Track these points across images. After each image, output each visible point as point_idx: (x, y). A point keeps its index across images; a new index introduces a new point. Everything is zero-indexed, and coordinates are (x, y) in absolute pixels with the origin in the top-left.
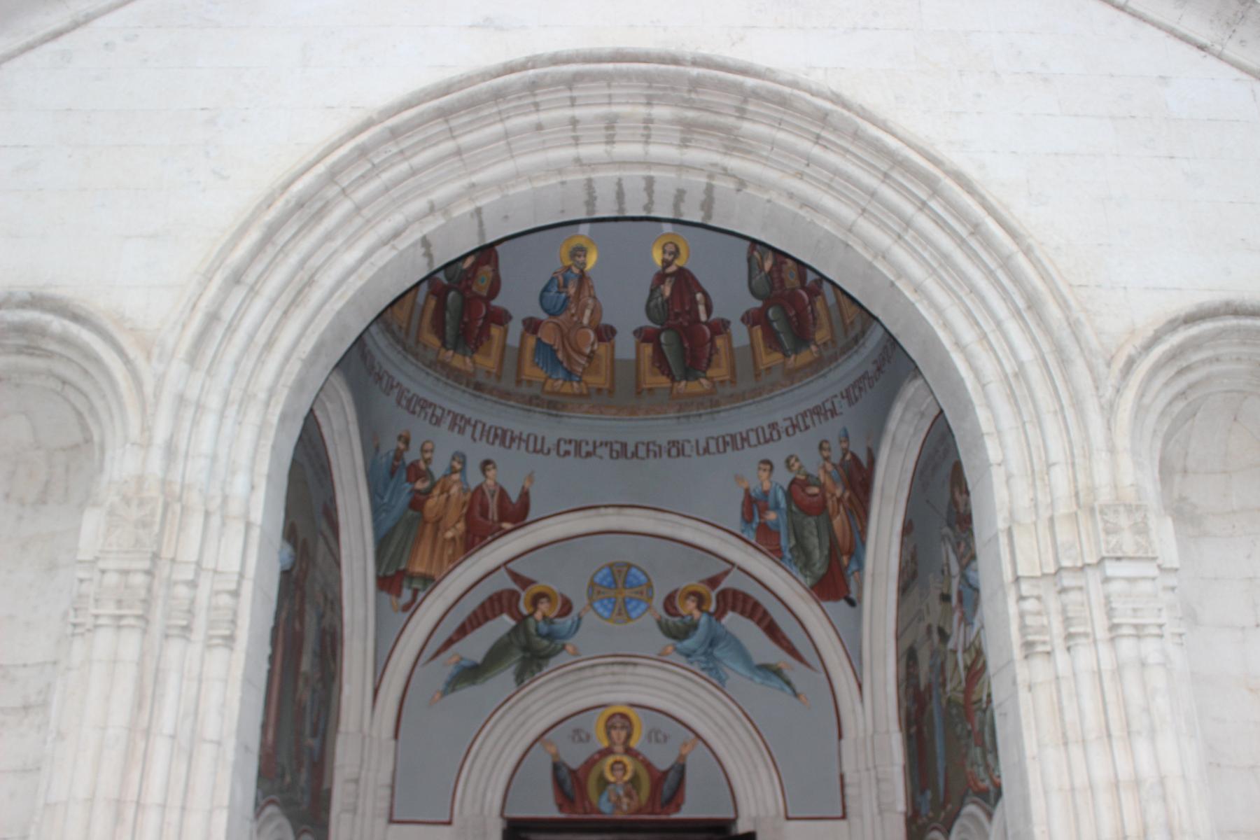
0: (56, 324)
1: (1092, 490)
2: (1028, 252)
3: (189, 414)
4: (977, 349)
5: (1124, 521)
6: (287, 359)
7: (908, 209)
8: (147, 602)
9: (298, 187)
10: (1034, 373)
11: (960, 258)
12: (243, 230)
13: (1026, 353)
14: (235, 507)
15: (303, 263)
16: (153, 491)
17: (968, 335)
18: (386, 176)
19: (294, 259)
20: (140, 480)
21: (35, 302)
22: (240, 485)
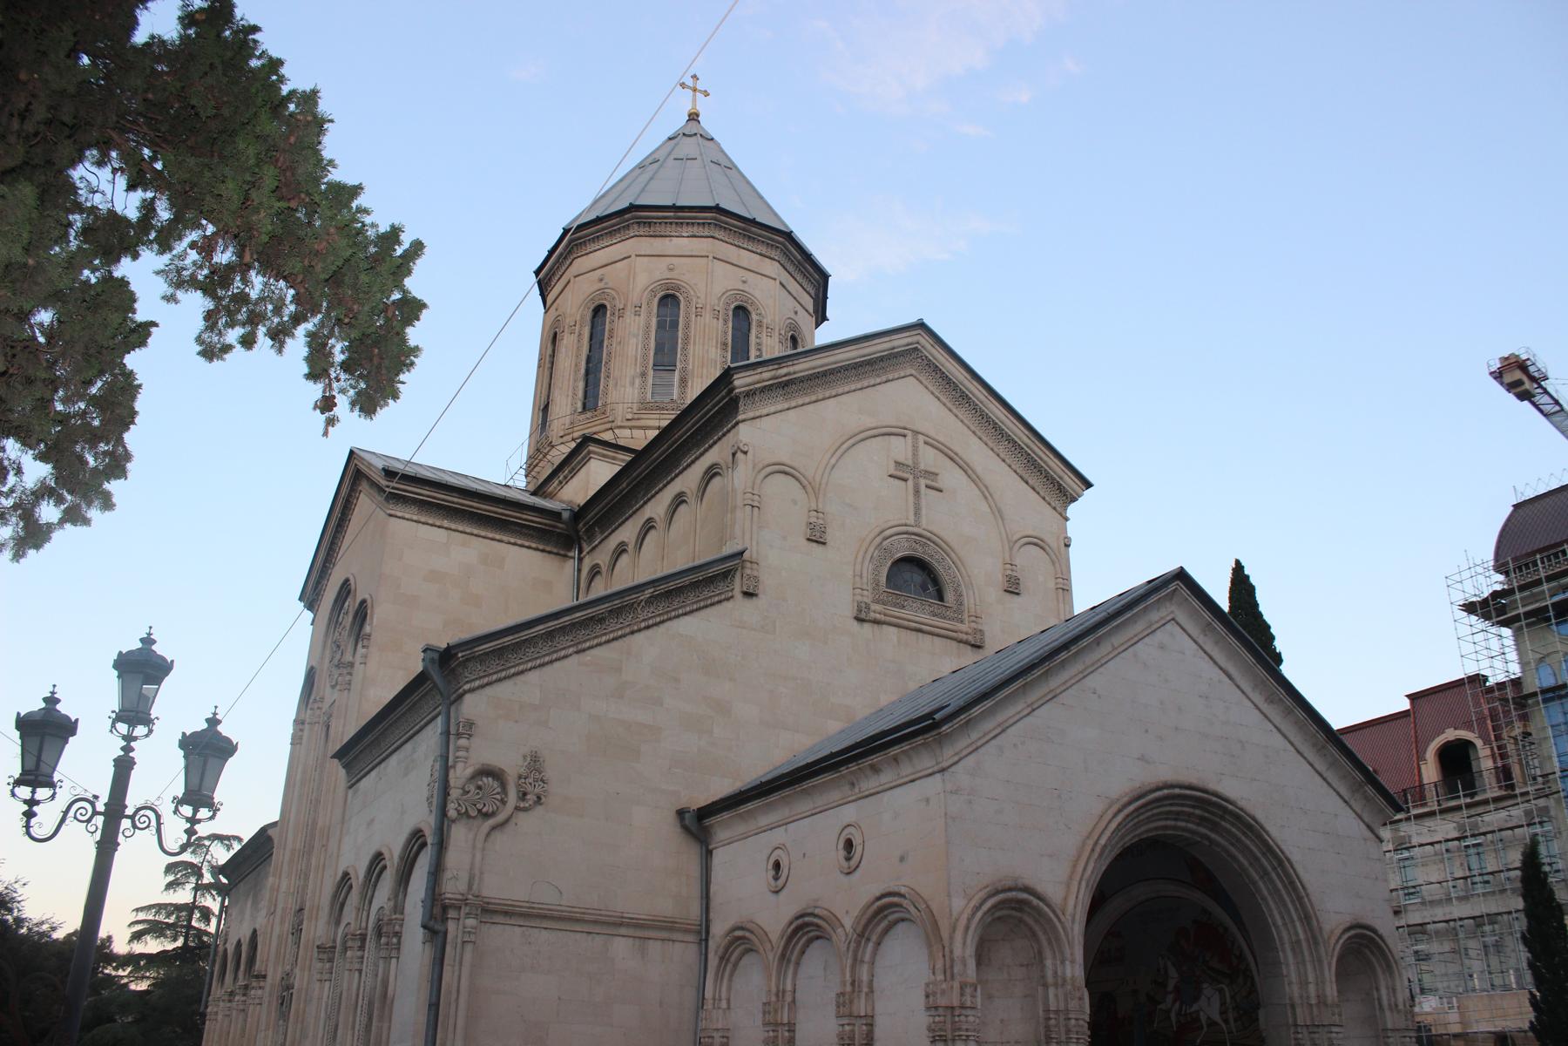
0: (1035, 901)
1: (1325, 996)
4: (1282, 928)
7: (1269, 868)
10: (1304, 944)
11: (1283, 892)
13: (1302, 936)
17: (1280, 922)
21: (1026, 889)
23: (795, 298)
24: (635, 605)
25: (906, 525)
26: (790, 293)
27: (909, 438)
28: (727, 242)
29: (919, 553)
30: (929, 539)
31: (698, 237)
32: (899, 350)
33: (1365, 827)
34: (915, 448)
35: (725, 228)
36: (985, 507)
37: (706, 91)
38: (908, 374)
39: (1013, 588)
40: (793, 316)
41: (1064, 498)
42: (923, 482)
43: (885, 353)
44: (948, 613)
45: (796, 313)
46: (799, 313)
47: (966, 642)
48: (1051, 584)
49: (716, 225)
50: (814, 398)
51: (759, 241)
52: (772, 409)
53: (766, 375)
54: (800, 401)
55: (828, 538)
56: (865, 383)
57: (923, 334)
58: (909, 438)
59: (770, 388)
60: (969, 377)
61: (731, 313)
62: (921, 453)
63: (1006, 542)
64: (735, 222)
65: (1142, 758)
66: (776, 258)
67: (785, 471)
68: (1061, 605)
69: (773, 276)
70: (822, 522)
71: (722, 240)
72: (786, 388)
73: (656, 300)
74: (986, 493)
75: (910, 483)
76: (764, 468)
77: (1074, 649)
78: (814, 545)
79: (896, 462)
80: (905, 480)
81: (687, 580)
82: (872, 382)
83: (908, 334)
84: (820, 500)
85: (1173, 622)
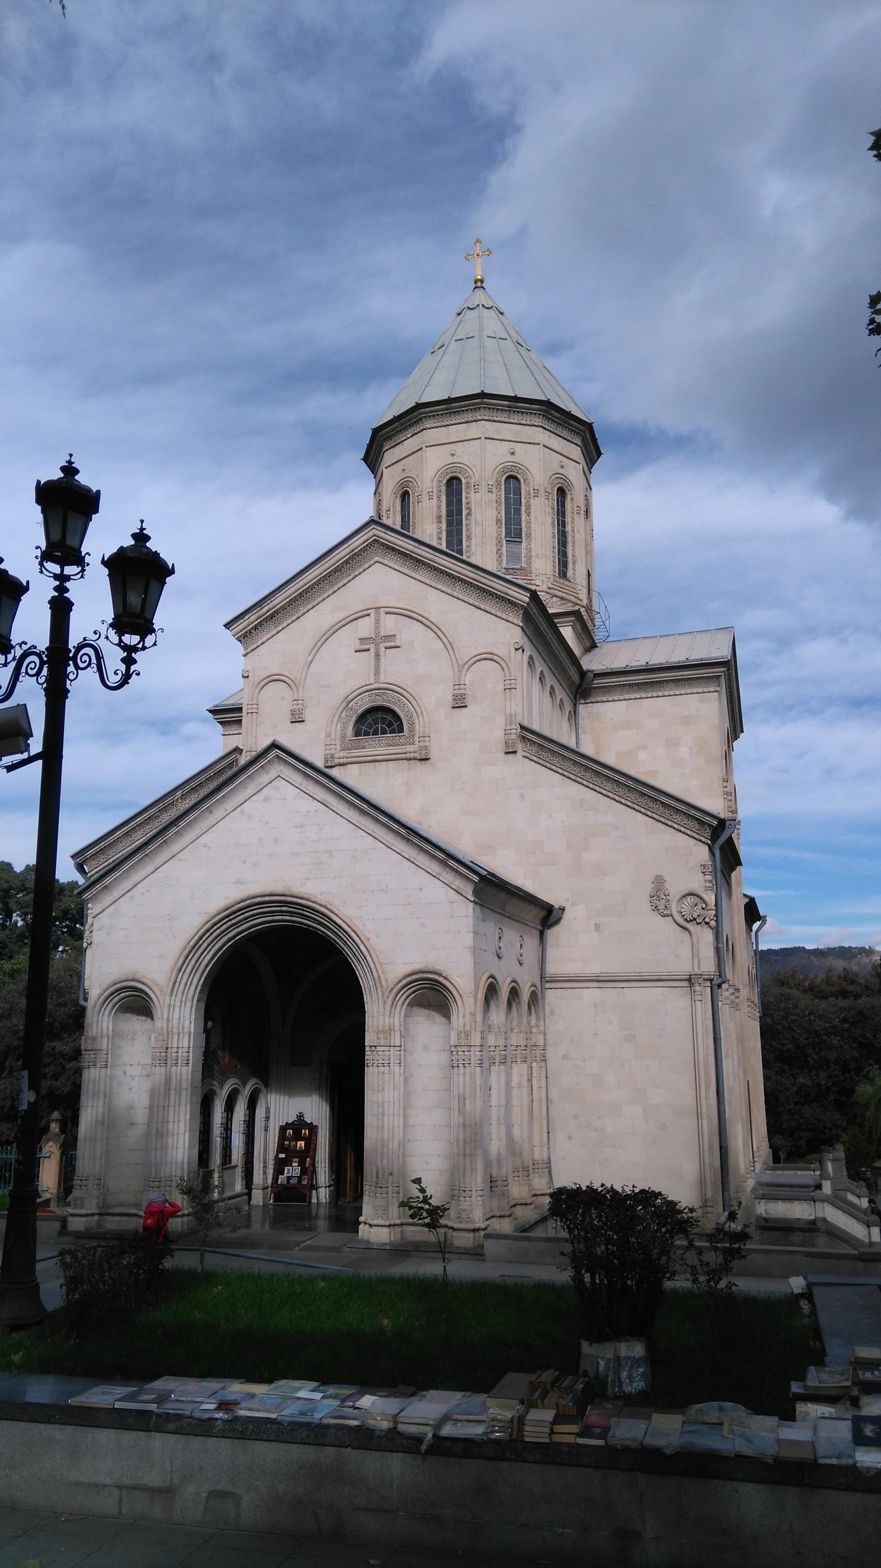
2: (370, 955)
3: (171, 1008)
5: (382, 1036)
6: (197, 987)
8: (166, 1060)
9: (192, 943)
10: (372, 988)
12: (180, 956)
14: (186, 1030)
15: (197, 962)
16: (165, 1032)
17: (362, 975)
18: (214, 935)
19: (193, 962)
20: (162, 1028)
22: (187, 1024)
23: (510, 441)
24: (175, 803)
25: (366, 685)
26: (501, 440)
27: (372, 616)
28: (437, 427)
29: (379, 703)
30: (387, 689)
31: (416, 434)
32: (359, 548)
33: (454, 892)
34: (377, 621)
35: (434, 416)
36: (440, 645)
37: (488, 250)
38: (372, 562)
39: (459, 703)
40: (511, 458)
41: (517, 608)
42: (382, 647)
43: (348, 557)
44: (401, 741)
45: (513, 453)
46: (517, 453)
47: (415, 759)
48: (501, 688)
49: (425, 417)
50: (294, 618)
51: (463, 411)
52: (264, 639)
53: (252, 619)
54: (285, 624)
55: (308, 715)
56: (335, 588)
57: (376, 527)
58: (372, 616)
59: (260, 624)
60: (416, 545)
61: (443, 489)
62: (382, 621)
63: (456, 666)
64: (438, 407)
65: (239, 882)
66: (480, 418)
67: (274, 679)
68: (508, 703)
69: (478, 437)
70: (300, 706)
71: (433, 428)
72: (274, 618)
73: (398, 502)
74: (439, 633)
75: (372, 651)
76: (259, 683)
77: (182, 824)
78: (297, 724)
79: (360, 639)
80: (369, 650)
81: (203, 778)
82: (340, 584)
83: (363, 533)
84: (301, 690)
85: (279, 778)
